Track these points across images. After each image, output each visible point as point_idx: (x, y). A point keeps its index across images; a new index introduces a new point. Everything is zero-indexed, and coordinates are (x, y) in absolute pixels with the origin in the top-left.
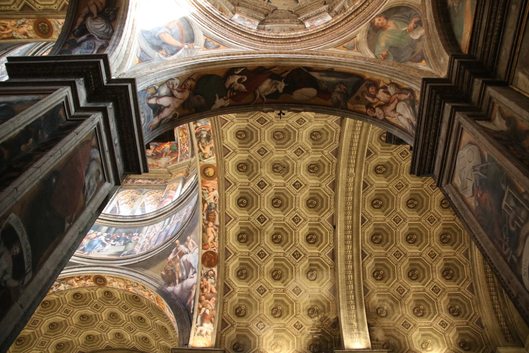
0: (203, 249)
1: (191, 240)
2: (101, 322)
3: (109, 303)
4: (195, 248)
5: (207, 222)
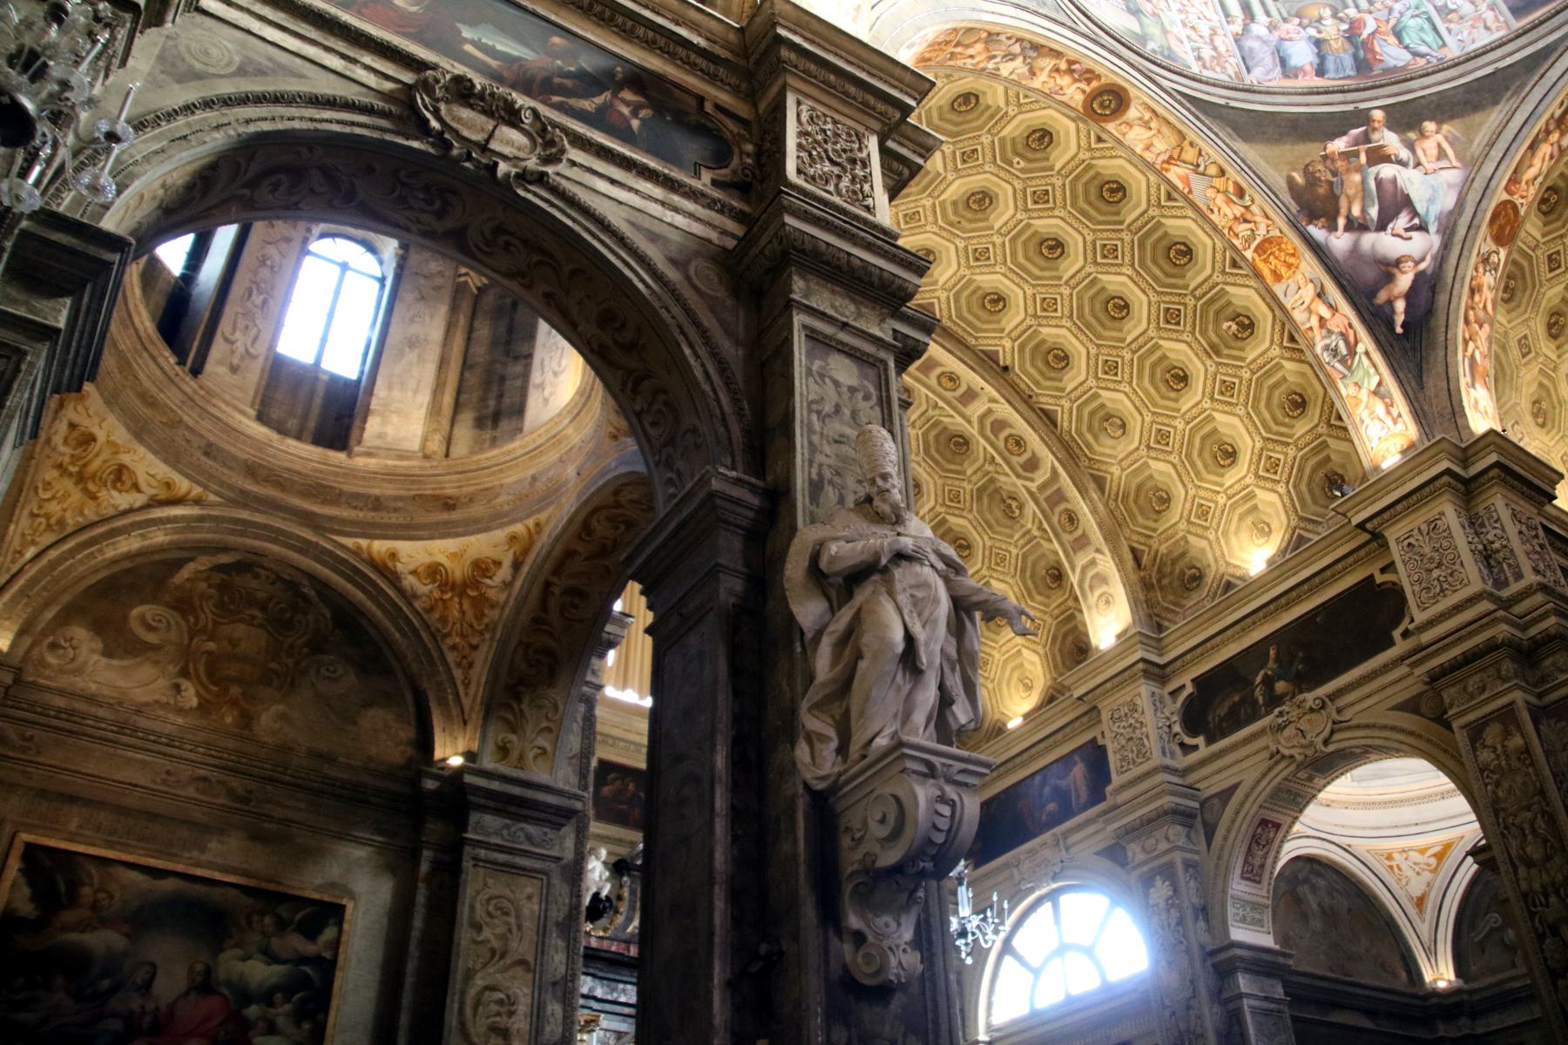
0: (1507, 189)
1: (1440, 138)
2: (928, 203)
4: (1444, 164)
5: (1552, 127)
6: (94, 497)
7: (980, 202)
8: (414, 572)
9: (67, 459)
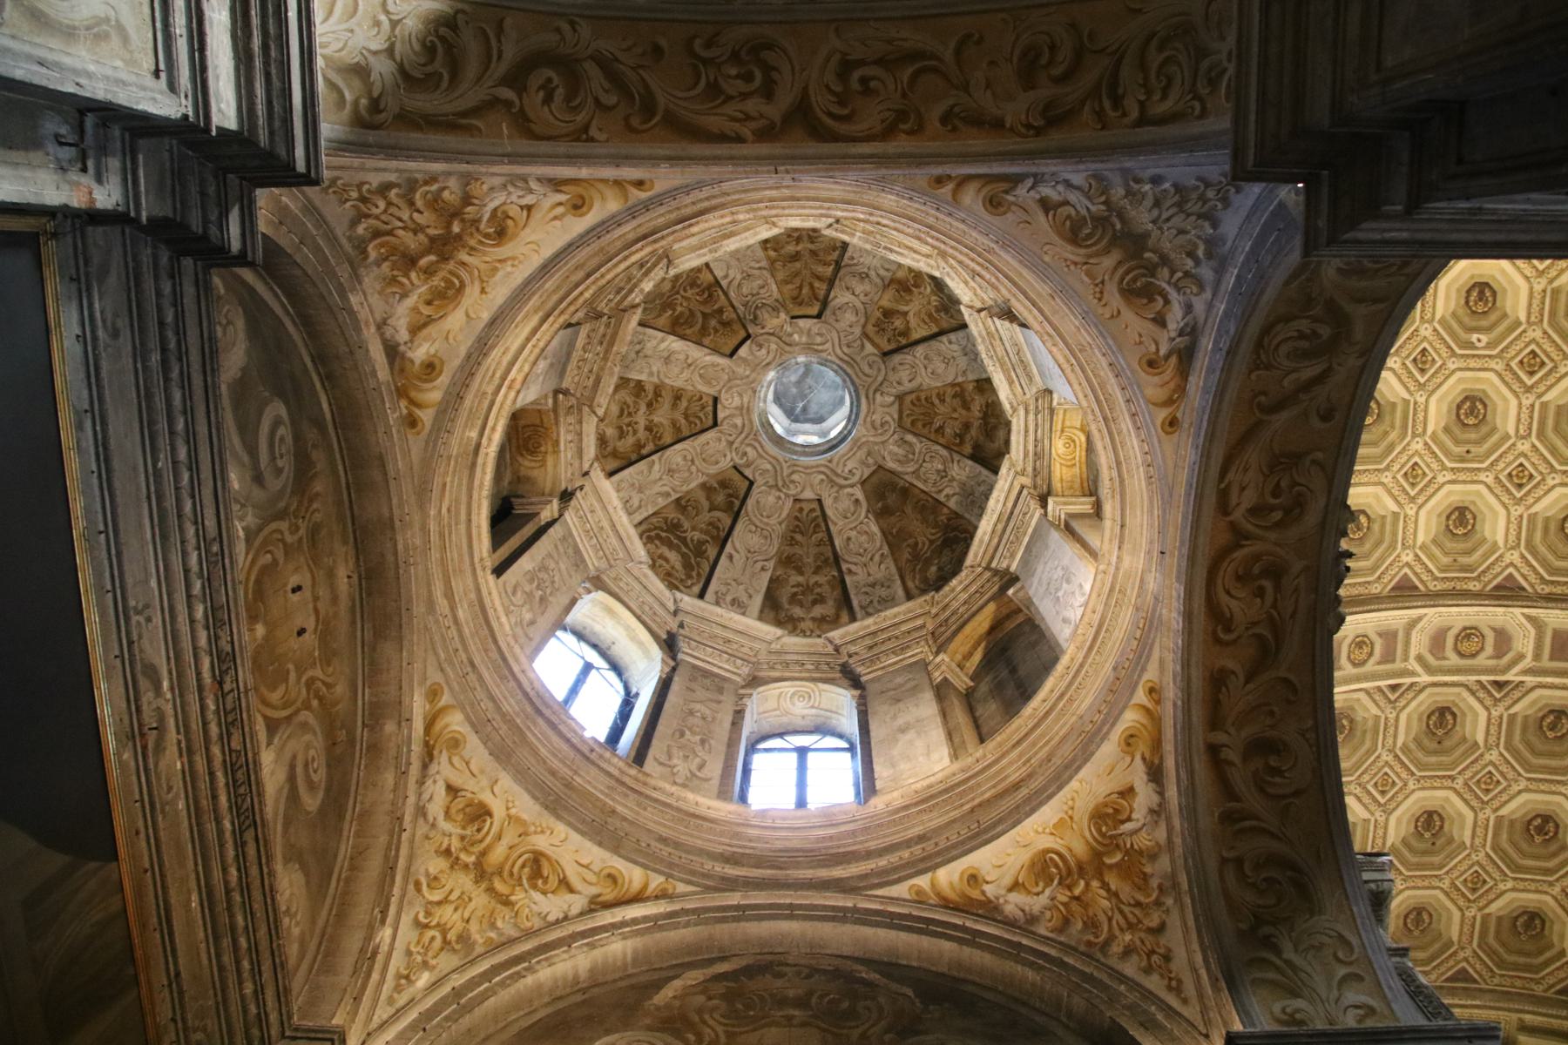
2: (1418, 445)
3: (1471, 346)
6: (507, 903)
7: (1472, 411)
8: (1015, 886)
9: (456, 844)
